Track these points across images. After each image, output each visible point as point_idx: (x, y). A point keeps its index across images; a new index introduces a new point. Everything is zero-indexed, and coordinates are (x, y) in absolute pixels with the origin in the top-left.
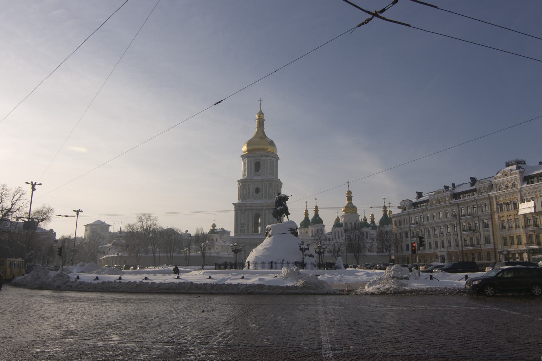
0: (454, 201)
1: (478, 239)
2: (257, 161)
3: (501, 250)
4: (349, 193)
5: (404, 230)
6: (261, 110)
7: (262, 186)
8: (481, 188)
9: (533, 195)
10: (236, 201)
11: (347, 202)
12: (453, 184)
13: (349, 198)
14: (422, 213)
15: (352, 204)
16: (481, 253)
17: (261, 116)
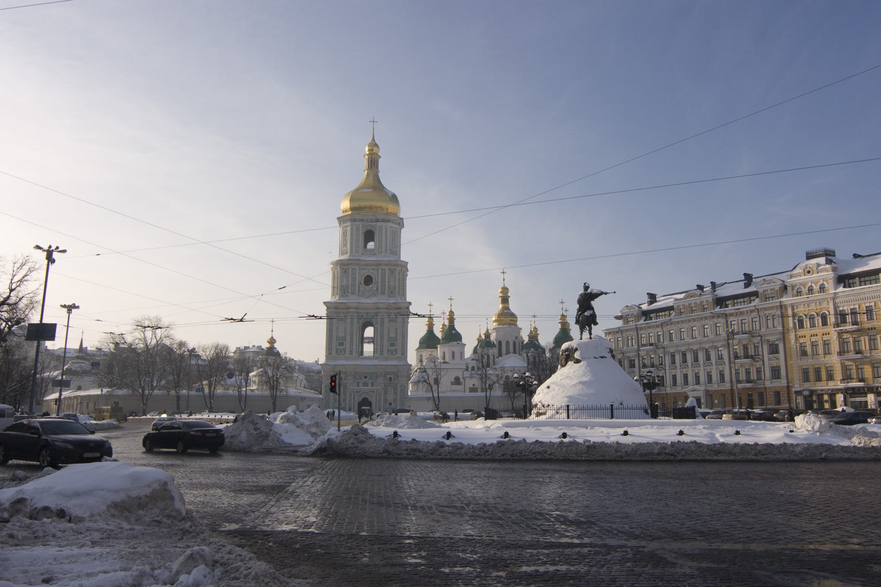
0: (718, 309)
1: (759, 371)
2: (369, 228)
3: (799, 389)
4: (505, 290)
5: (627, 355)
6: (373, 139)
7: (378, 273)
8: (767, 290)
9: (854, 305)
10: (328, 297)
11: (501, 306)
12: (712, 283)
13: (505, 300)
14: (660, 328)
15: (509, 310)
16: (765, 394)
17: (375, 150)
